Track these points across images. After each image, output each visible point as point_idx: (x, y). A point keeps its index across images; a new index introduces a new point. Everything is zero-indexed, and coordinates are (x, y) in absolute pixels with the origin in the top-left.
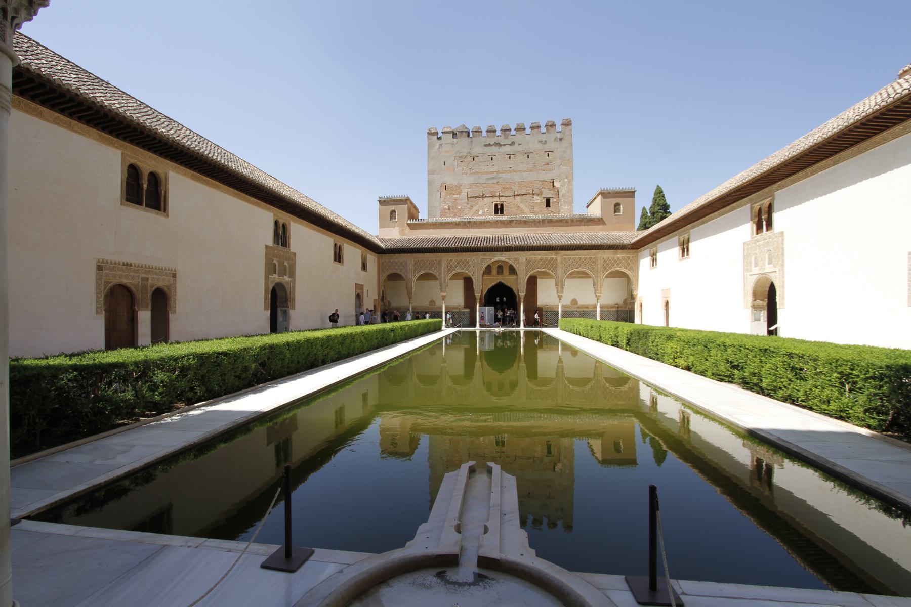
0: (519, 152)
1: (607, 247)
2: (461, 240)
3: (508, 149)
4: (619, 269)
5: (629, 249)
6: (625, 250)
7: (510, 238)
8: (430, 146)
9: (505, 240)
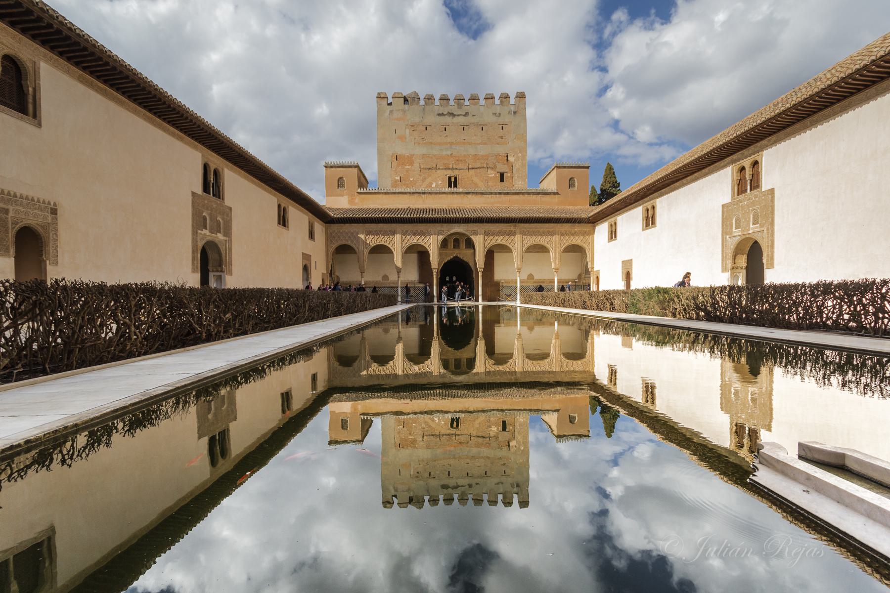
0: (473, 123)
3: (461, 120)
4: (576, 243)
8: (380, 112)
9: (462, 212)
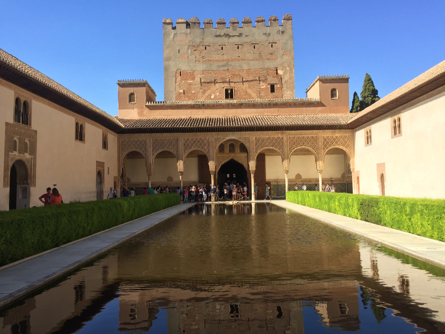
1: (326, 127)
2: (196, 121)
3: (236, 40)
4: (337, 146)
5: (345, 129)
6: (341, 130)
7: (240, 119)
9: (236, 121)
